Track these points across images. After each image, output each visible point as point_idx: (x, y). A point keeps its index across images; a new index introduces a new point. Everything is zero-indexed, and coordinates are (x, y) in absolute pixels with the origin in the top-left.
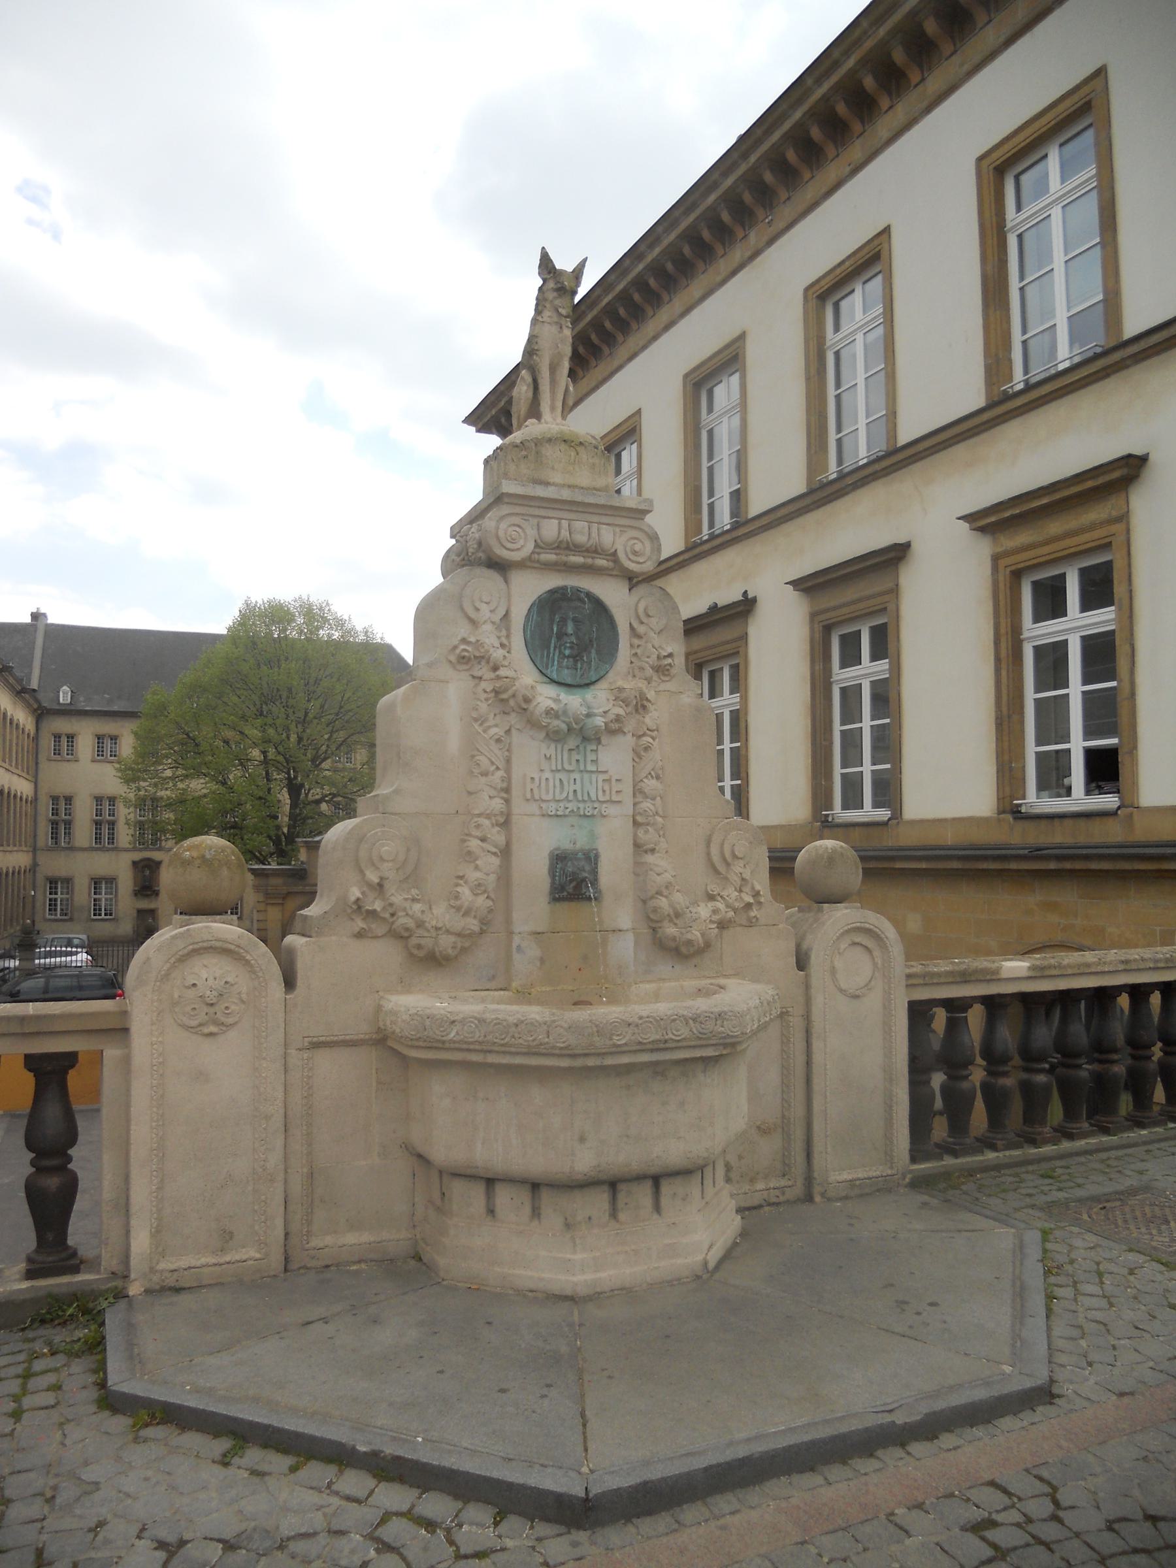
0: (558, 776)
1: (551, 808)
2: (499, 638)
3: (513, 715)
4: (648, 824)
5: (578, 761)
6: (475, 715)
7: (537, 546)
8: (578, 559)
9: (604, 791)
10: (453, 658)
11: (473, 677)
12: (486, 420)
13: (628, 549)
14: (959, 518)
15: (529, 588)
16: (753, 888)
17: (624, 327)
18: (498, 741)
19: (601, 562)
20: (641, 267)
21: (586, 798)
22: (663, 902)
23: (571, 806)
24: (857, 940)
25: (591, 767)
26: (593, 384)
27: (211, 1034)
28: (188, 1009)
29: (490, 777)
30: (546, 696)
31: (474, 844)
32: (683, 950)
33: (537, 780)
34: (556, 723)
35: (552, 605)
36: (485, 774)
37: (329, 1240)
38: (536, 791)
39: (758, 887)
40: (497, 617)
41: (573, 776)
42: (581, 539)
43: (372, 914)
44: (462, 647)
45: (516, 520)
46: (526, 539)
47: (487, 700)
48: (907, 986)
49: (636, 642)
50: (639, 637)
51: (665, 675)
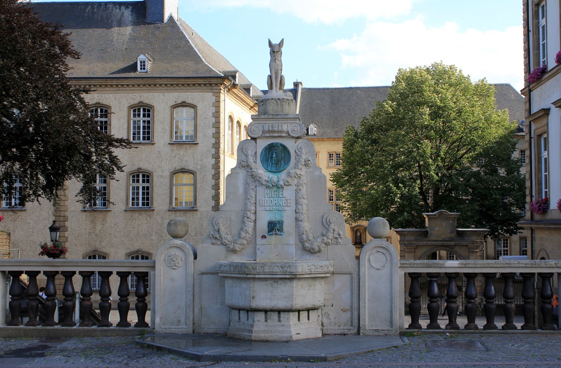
0: (270, 199)
7: (263, 132)
15: (262, 144)
19: (284, 135)
23: (274, 208)
32: (312, 251)
35: (270, 148)
41: (275, 199)
45: (256, 125)
49: (297, 157)
50: (298, 156)
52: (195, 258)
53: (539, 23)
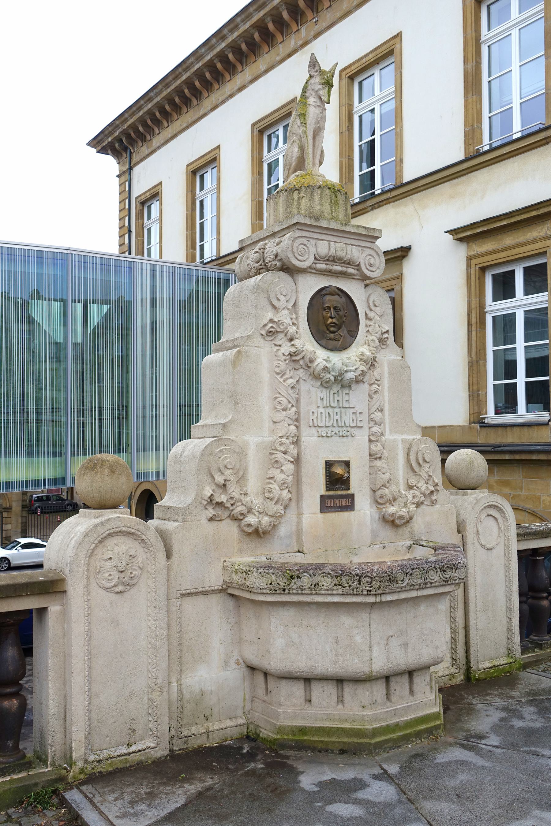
1: (323, 431)
2: (291, 319)
3: (302, 370)
4: (377, 441)
5: (338, 400)
6: (277, 370)
7: (315, 258)
8: (338, 268)
9: (353, 420)
10: (264, 332)
11: (276, 345)
12: (104, 144)
13: (367, 262)
14: (446, 232)
15: (310, 286)
16: (434, 481)
17: (208, 86)
18: (292, 387)
19: (351, 270)
20: (223, 45)
21: (343, 425)
22: (386, 491)
23: (336, 430)
24: (490, 513)
25: (346, 405)
26: (185, 125)
27: (121, 592)
28: (107, 575)
29: (288, 411)
30: (322, 356)
31: (279, 456)
32: (398, 522)
33: (316, 414)
34: (328, 376)
36: (284, 410)
37: (194, 730)
38: (315, 421)
39: (436, 481)
40: (290, 306)
42: (341, 254)
43: (220, 504)
44: (271, 325)
45: (304, 241)
46: (309, 254)
47: (285, 360)
48: (517, 541)
49: (369, 323)
51: (383, 345)
52: (169, 555)
53: (143, 224)
